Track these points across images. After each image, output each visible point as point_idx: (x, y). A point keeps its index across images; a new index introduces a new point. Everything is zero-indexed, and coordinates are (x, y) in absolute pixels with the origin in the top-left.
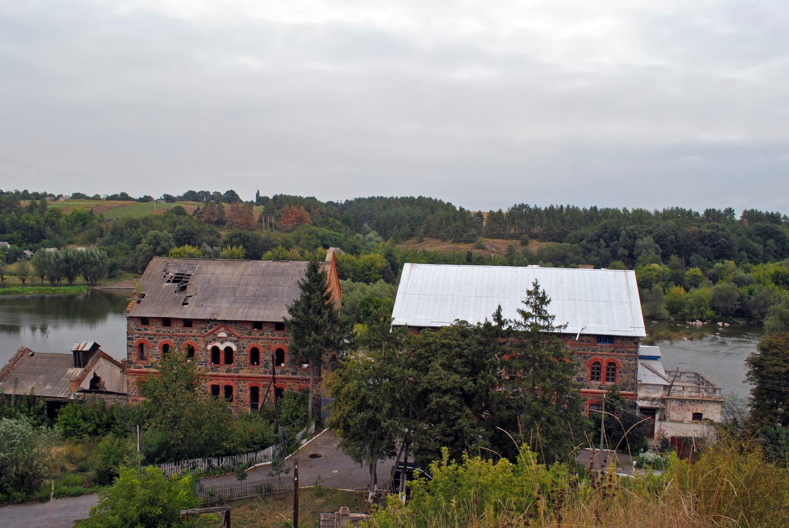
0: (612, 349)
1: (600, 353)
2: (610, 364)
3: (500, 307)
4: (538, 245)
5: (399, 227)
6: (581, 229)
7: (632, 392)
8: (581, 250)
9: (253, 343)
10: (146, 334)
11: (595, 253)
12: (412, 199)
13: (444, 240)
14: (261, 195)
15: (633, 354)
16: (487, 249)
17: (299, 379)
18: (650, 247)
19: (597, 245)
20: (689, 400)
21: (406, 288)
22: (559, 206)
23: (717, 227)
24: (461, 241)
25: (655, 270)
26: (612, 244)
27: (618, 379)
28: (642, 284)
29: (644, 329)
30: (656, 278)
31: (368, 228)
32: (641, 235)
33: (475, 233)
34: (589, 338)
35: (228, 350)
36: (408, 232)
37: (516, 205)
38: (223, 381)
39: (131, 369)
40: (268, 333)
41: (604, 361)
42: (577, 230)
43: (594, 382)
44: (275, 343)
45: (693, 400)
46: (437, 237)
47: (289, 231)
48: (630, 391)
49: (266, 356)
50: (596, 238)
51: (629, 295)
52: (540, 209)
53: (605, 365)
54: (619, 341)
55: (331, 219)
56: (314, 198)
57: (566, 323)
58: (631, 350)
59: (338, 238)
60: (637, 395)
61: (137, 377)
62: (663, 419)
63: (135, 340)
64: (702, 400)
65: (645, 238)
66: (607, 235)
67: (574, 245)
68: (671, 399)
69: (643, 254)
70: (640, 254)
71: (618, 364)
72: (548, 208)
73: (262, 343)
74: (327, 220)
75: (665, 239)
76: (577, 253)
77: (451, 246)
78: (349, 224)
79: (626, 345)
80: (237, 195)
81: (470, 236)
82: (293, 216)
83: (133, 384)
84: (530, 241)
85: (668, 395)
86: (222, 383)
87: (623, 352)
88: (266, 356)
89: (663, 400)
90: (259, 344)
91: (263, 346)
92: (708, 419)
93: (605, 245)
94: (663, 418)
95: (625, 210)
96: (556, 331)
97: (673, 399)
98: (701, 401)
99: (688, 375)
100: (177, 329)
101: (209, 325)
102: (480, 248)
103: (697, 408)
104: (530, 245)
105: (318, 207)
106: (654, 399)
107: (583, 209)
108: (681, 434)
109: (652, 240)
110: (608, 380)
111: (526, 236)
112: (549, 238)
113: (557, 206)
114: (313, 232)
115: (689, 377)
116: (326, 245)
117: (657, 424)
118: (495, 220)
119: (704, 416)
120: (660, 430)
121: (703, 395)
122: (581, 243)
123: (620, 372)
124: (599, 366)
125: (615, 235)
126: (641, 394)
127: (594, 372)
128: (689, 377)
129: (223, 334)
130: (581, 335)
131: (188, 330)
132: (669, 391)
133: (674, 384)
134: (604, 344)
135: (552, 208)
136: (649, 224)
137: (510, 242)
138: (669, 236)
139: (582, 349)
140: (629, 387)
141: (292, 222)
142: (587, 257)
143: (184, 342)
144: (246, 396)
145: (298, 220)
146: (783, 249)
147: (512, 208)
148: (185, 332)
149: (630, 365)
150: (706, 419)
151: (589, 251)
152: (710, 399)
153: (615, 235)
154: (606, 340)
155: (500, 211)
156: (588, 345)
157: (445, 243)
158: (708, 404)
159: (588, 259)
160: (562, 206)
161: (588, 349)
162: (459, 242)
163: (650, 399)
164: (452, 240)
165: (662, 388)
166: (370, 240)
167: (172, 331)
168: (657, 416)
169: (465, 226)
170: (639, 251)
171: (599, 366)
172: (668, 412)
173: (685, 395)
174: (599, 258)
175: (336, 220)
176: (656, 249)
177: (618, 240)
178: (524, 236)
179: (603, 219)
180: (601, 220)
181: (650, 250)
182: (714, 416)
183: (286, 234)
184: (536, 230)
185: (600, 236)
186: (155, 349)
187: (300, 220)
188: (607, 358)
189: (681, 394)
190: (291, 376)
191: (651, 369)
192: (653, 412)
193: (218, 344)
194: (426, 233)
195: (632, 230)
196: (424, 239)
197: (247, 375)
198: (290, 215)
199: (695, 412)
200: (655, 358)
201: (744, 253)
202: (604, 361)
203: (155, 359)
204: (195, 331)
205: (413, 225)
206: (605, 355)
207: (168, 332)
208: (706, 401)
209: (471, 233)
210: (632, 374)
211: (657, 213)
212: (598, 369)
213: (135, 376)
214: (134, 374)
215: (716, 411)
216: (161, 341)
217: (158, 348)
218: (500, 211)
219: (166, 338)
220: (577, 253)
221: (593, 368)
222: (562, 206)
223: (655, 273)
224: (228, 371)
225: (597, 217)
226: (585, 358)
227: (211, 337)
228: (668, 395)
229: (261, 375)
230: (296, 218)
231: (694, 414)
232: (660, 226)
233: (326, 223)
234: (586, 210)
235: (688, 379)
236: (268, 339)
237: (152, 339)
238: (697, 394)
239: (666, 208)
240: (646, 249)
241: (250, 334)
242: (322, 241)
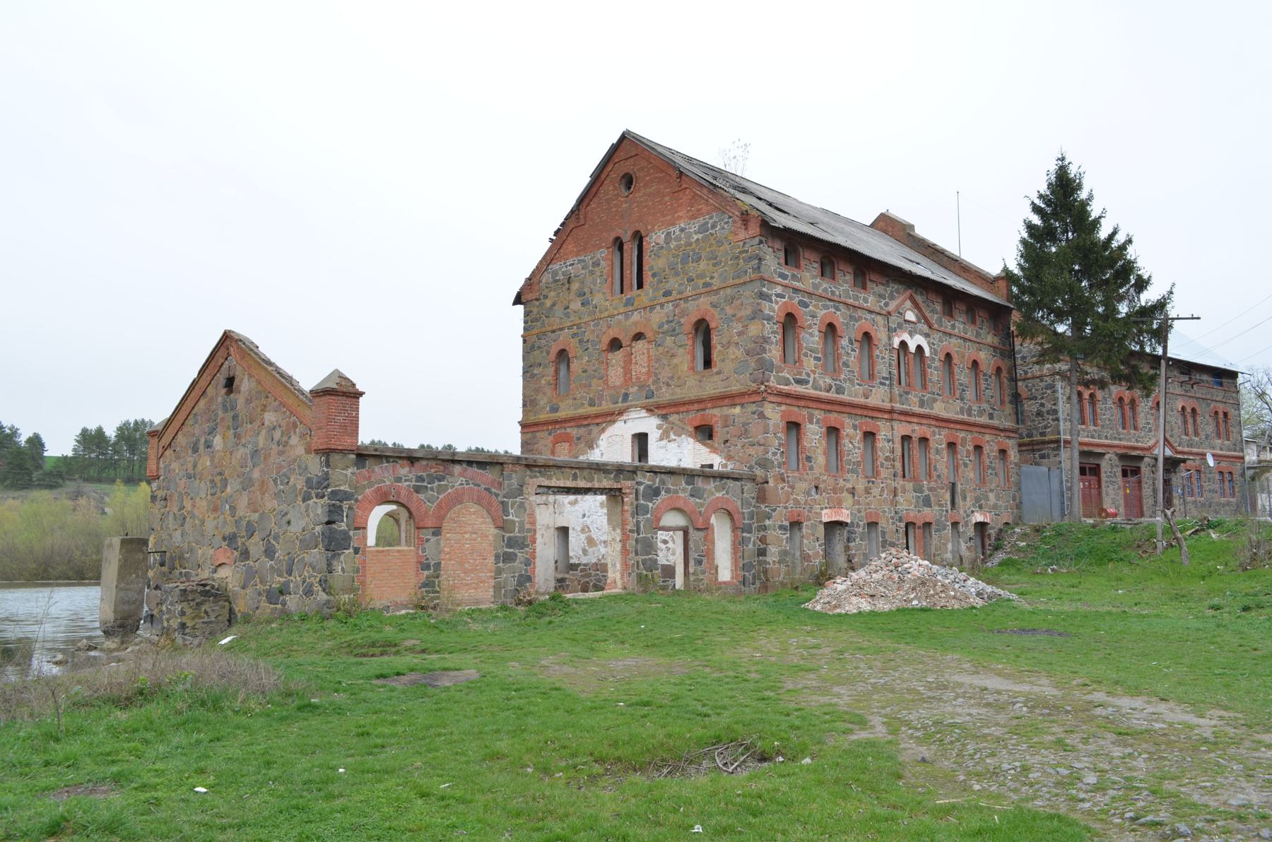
10: (796, 290)
17: (997, 429)
38: (916, 427)
39: (771, 384)
44: (969, 349)
61: (783, 408)
63: (777, 303)
73: (955, 345)
83: (776, 425)
86: (917, 430)
91: (957, 352)
101: (889, 289)
129: (910, 316)
143: (857, 324)
148: (857, 298)
167: (837, 293)
186: (811, 334)
193: (906, 337)
197: (945, 415)
203: (812, 361)
207: (833, 292)
213: (780, 404)
214: (779, 400)
217: (817, 333)
219: (826, 307)
229: (960, 417)
236: (961, 338)
237: (806, 306)
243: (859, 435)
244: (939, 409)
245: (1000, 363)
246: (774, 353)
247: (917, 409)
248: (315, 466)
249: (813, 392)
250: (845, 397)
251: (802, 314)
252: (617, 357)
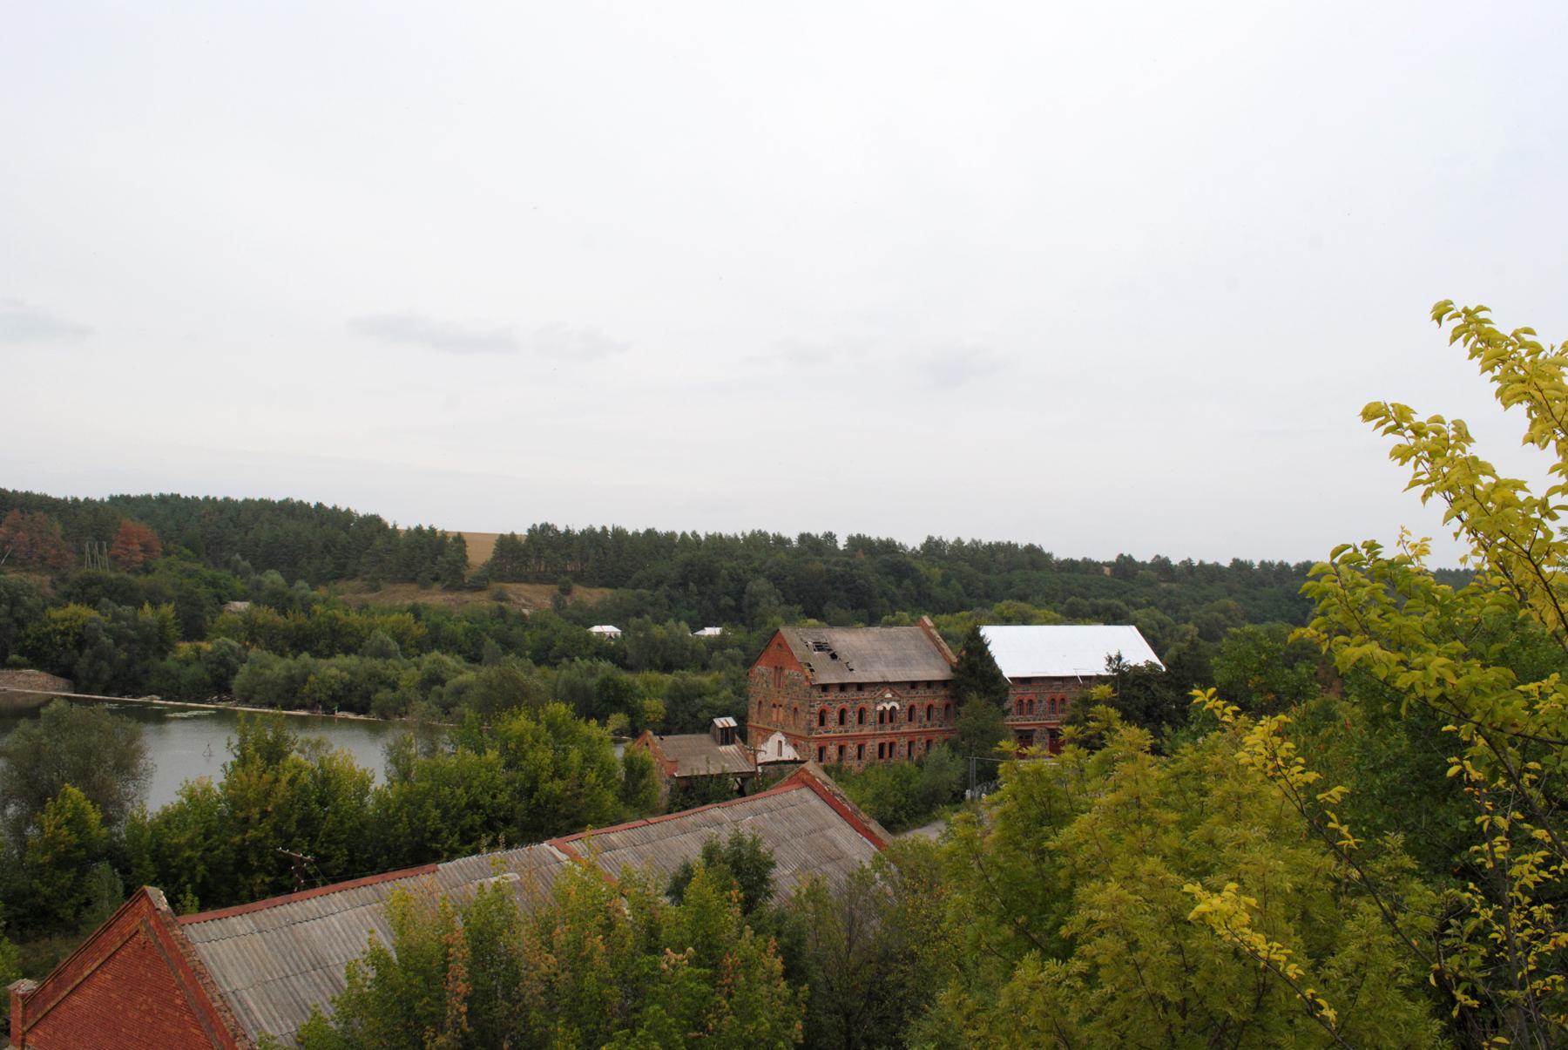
9: (911, 702)
23: (848, 563)
35: (894, 708)
37: (534, 525)
40: (922, 691)
49: (921, 712)
50: (680, 581)
86: (887, 740)
88: (921, 712)
90: (915, 702)
100: (852, 694)
129: (889, 695)
131: (861, 693)
144: (905, 751)
146: (919, 593)
190: (938, 728)
197: (908, 730)
201: (885, 600)
204: (866, 694)
205: (339, 559)
216: (839, 706)
224: (893, 729)
227: (880, 698)
241: (908, 693)
243: (856, 746)
244: (904, 729)
245: (949, 701)
246: (815, 724)
247: (889, 732)
248: (668, 778)
249: (831, 735)
250: (850, 734)
251: (829, 709)
252: (775, 710)
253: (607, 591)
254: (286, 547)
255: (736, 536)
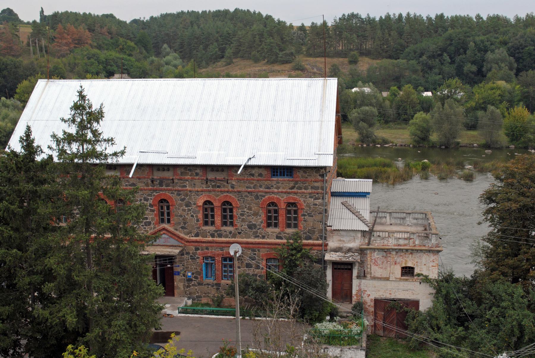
0: (292, 184)
1: (276, 190)
2: (289, 204)
3: (29, 128)
4: (369, 64)
5: (206, 47)
6: (421, 42)
7: (320, 242)
8: (419, 68)
11: (437, 71)
12: (226, 12)
13: (256, 61)
14: (46, 13)
15: (320, 191)
16: (306, 69)
18: (503, 61)
19: (440, 61)
20: (396, 249)
21: (33, 112)
22: (397, 15)
24: (277, 62)
25: (499, 88)
26: (458, 59)
27: (301, 225)
28: (483, 106)
29: (332, 157)
30: (500, 98)
31: (168, 49)
32: (493, 47)
33: (293, 51)
34: (261, 171)
36: (216, 53)
37: (344, 15)
41: (282, 200)
42: (417, 43)
43: (270, 230)
45: (400, 249)
46: (249, 58)
47: (63, 56)
48: (317, 239)
50: (439, 52)
51: (322, 111)
52: (374, 19)
53: (283, 206)
54: (179, 171)
55: (121, 40)
56: (111, 16)
57: (123, 149)
58: (316, 184)
59: (126, 63)
60: (326, 245)
62: (362, 276)
64: (412, 250)
65: (496, 51)
66: (453, 48)
67: (411, 62)
68: (371, 249)
69: (494, 70)
70: (490, 70)
71: (301, 205)
72: (384, 18)
74: (117, 42)
75: (521, 51)
76: (415, 71)
77: (264, 68)
78: (145, 47)
79: (309, 179)
80: (16, 15)
81: (286, 55)
82: (69, 37)
84: (360, 59)
85: (369, 244)
87: (306, 188)
89: (361, 251)
92: (422, 275)
93: (450, 61)
94: (362, 275)
95: (478, 17)
96: (110, 161)
97: (374, 250)
98: (412, 251)
99: (416, 216)
102: (298, 69)
103: (406, 261)
104: (360, 63)
105: (106, 25)
106: (350, 250)
107: (427, 17)
108: (387, 296)
109: (505, 52)
110: (289, 226)
111: (355, 52)
112: (384, 54)
113: (394, 14)
114: (94, 55)
115: (417, 219)
116: (110, 72)
117: (355, 282)
118: (318, 34)
119: (416, 271)
120: (360, 291)
121: (414, 243)
122: (421, 59)
123: (304, 215)
124: (276, 208)
125: (462, 48)
126: (332, 244)
127: (271, 216)
128: (417, 219)
130: (246, 167)
132: (370, 239)
133: (377, 228)
134: (281, 179)
135: (388, 17)
136: (504, 34)
137: (336, 61)
138: (526, 46)
139: (252, 186)
140: (317, 234)
141: (67, 44)
142: (427, 76)
145: (76, 42)
147: (340, 19)
149: (316, 205)
150: (419, 275)
151: (431, 68)
152: (424, 248)
153: (462, 48)
154: (284, 172)
155: (325, 23)
156: (261, 180)
157: (257, 65)
158: (421, 254)
159: (428, 78)
160: (400, 15)
161: (261, 186)
162: (274, 62)
163: (353, 250)
164: (266, 60)
165: (359, 235)
166: (167, 64)
168: (355, 272)
169: (283, 43)
170: (489, 66)
171: (276, 208)
172: (369, 266)
173: (391, 243)
174: (441, 76)
175: (129, 41)
176: (510, 63)
177: (465, 54)
178: (352, 53)
179: (450, 29)
180: (447, 30)
181: (503, 65)
182: (429, 270)
183: (59, 60)
184: (368, 45)
185: (444, 50)
187: (79, 42)
188: (285, 196)
189: (386, 242)
191: (352, 209)
192: (350, 267)
194: (236, 54)
195: (482, 41)
196: (234, 60)
198: (66, 35)
199: (404, 265)
200: (363, 195)
202: (282, 200)
205: (222, 45)
206: (282, 192)
208: (417, 250)
209: (287, 52)
210: (318, 217)
211: (518, 20)
212: (276, 211)
215: (431, 264)
218: (325, 23)
220: (415, 71)
221: (269, 211)
222: (400, 15)
223: (498, 92)
225: (444, 27)
226: (257, 197)
228: (369, 244)
230: (74, 40)
231: (403, 268)
232: (517, 35)
233: (115, 45)
234: (431, 18)
235: (415, 221)
238: (406, 242)
239: (529, 13)
240: (497, 63)
242: (105, 67)
253: (386, 62)
254: (197, 39)
255: (465, 16)
